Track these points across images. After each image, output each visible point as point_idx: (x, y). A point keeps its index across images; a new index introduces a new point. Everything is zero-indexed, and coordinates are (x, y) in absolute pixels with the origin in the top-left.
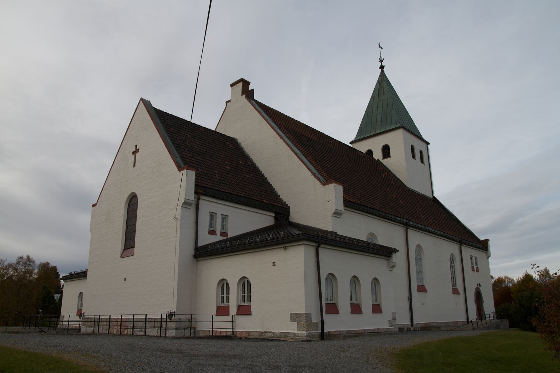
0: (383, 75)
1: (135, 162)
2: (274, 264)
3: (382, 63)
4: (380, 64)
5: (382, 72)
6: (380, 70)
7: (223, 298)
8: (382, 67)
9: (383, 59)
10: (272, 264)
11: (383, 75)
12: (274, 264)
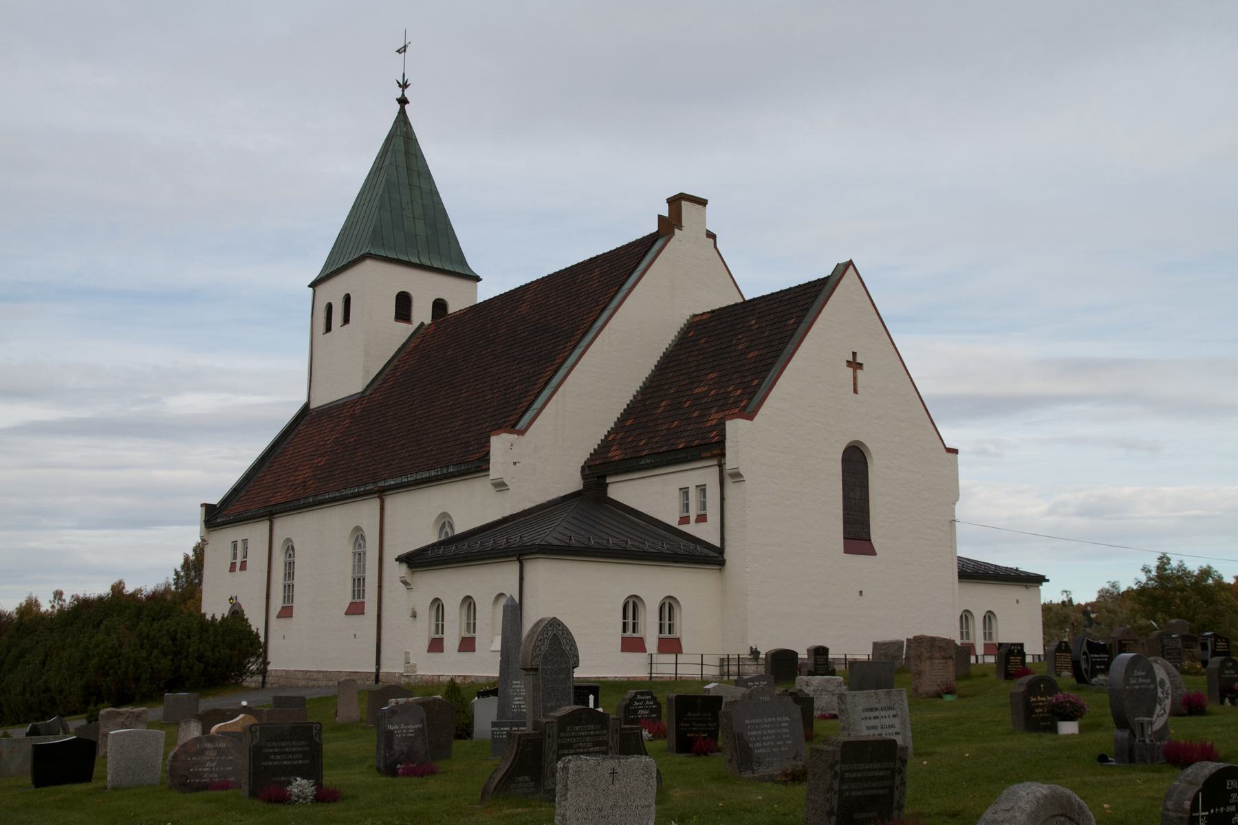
0: (402, 119)
1: (855, 384)
2: (1018, 602)
3: (403, 91)
4: (398, 93)
5: (402, 112)
6: (399, 106)
8: (403, 101)
9: (409, 85)
11: (402, 119)
12: (1018, 602)
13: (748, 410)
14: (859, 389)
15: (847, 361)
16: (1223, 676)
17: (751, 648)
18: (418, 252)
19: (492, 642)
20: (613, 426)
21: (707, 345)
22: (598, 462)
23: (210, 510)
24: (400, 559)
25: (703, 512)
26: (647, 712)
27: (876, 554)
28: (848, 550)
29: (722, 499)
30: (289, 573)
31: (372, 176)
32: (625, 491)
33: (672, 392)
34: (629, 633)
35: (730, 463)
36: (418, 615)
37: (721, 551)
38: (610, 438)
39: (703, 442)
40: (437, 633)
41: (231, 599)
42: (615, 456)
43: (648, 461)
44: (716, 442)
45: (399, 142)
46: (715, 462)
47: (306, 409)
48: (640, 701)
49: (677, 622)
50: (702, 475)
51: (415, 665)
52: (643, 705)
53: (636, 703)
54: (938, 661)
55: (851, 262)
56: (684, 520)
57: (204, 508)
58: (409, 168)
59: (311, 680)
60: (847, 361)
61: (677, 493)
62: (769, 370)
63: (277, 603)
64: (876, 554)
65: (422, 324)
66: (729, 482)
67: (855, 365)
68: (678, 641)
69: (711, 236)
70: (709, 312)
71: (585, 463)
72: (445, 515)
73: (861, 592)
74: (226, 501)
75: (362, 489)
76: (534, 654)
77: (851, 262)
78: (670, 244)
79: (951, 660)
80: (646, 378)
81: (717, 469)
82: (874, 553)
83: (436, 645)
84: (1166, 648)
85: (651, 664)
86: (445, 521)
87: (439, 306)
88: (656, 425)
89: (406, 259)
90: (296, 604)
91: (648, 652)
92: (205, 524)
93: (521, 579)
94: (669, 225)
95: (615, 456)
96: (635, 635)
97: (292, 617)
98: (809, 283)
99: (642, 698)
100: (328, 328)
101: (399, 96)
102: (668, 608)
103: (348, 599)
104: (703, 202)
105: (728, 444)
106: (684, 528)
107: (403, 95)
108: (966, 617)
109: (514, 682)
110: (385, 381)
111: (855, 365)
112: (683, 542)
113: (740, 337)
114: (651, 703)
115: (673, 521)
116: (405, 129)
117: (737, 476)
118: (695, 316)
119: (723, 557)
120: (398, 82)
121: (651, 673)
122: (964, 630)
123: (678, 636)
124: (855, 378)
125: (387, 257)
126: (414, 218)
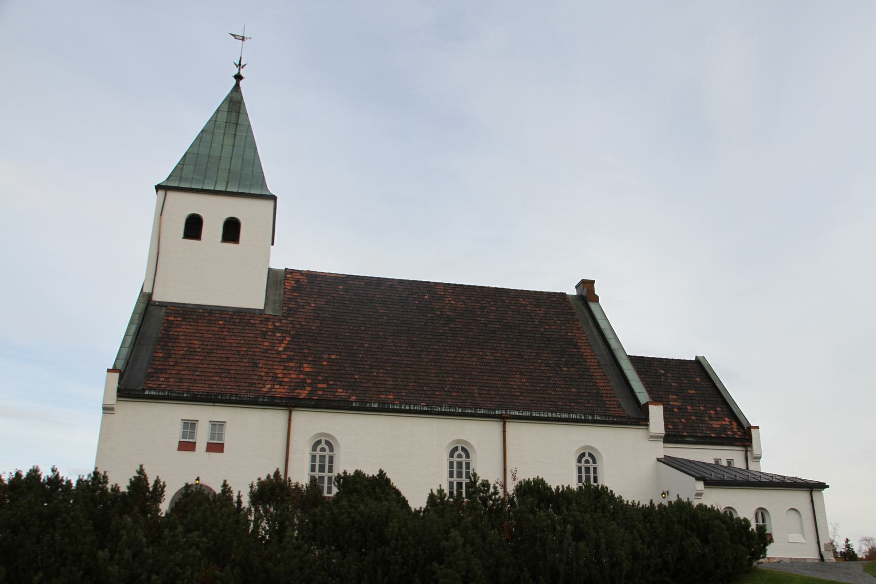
3: (239, 70)
5: (237, 87)
8: (238, 77)
9: (245, 65)
101: (236, 72)
107: (239, 73)
120: (235, 64)
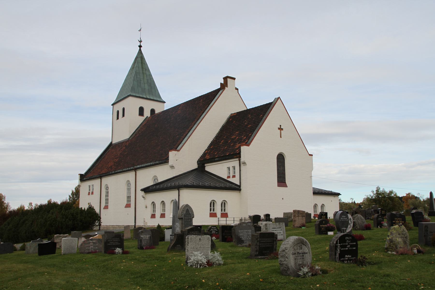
0: (140, 52)
1: (281, 135)
2: (332, 201)
3: (140, 44)
5: (140, 50)
6: (139, 48)
7: (314, 211)
8: (140, 46)
10: (331, 201)
11: (140, 52)
12: (332, 201)
13: (248, 143)
14: (282, 136)
15: (278, 128)
16: (378, 220)
17: (249, 216)
18: (146, 94)
19: (170, 215)
20: (207, 148)
21: (235, 123)
22: (202, 159)
23: (81, 176)
24: (142, 190)
25: (234, 175)
26: (215, 232)
27: (287, 187)
28: (279, 186)
29: (240, 170)
30: (107, 196)
31: (131, 70)
32: (211, 168)
33: (225, 137)
34: (212, 212)
35: (242, 159)
36: (147, 207)
37: (240, 186)
38: (206, 152)
39: (234, 153)
40: (153, 212)
41: (89, 203)
42: (207, 158)
43: (217, 159)
44: (238, 153)
45: (139, 59)
46: (238, 159)
47: (111, 144)
48: (212, 229)
49: (226, 208)
50: (234, 163)
51: (147, 222)
52: (214, 230)
53: (211, 229)
54: (300, 217)
55: (279, 98)
56: (229, 177)
57: (80, 175)
58: (142, 68)
59: (114, 228)
60: (278, 128)
61: (226, 169)
62: (254, 131)
63: (103, 205)
64: (287, 187)
65: (147, 117)
66: (242, 165)
67: (280, 129)
68: (227, 214)
69: (237, 89)
70: (236, 113)
71: (198, 160)
72: (155, 176)
73: (283, 198)
74: (86, 173)
75: (129, 169)
76: (182, 214)
77: (279, 98)
78: (224, 92)
79: (304, 217)
80: (217, 133)
81: (238, 161)
82: (287, 187)
83: (153, 216)
84: (366, 213)
85: (219, 221)
86: (155, 178)
87: (153, 111)
88: (220, 148)
89: (142, 96)
90: (109, 205)
91: (218, 217)
92: (80, 180)
93: (179, 195)
94: (224, 86)
95: (207, 158)
96: (214, 212)
97: (108, 209)
98: (267, 104)
99: (213, 228)
100: (118, 118)
101: (139, 45)
102: (224, 204)
103: (126, 203)
104: (234, 79)
105: (242, 154)
106: (229, 179)
107: (140, 44)
108: (315, 206)
109: (176, 223)
110: (136, 135)
111: (280, 129)
112: (228, 184)
113: (245, 120)
114: (216, 229)
115: (225, 177)
116: (141, 55)
117: (244, 163)
118: (232, 114)
119: (240, 188)
120: (139, 40)
121: (219, 224)
122: (315, 210)
123: (227, 212)
124: (281, 133)
125: (136, 96)
126: (144, 83)
